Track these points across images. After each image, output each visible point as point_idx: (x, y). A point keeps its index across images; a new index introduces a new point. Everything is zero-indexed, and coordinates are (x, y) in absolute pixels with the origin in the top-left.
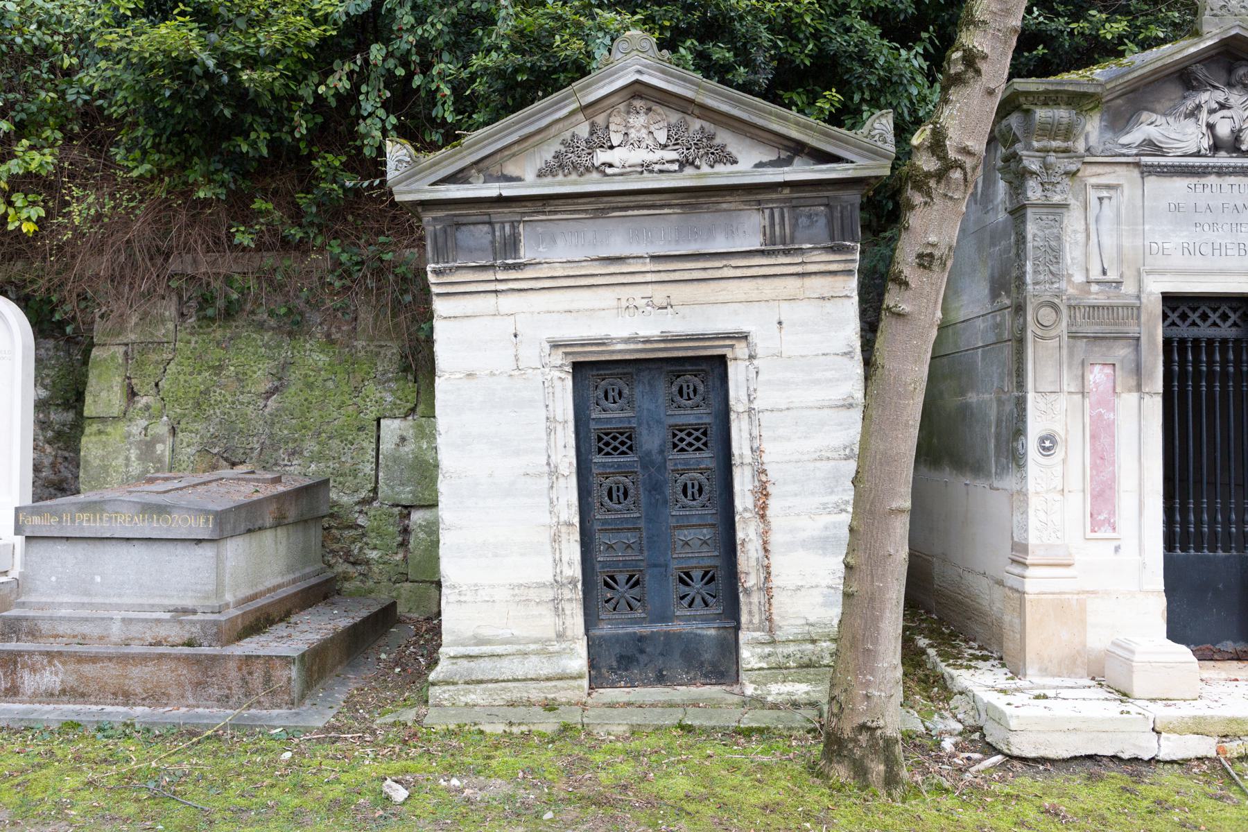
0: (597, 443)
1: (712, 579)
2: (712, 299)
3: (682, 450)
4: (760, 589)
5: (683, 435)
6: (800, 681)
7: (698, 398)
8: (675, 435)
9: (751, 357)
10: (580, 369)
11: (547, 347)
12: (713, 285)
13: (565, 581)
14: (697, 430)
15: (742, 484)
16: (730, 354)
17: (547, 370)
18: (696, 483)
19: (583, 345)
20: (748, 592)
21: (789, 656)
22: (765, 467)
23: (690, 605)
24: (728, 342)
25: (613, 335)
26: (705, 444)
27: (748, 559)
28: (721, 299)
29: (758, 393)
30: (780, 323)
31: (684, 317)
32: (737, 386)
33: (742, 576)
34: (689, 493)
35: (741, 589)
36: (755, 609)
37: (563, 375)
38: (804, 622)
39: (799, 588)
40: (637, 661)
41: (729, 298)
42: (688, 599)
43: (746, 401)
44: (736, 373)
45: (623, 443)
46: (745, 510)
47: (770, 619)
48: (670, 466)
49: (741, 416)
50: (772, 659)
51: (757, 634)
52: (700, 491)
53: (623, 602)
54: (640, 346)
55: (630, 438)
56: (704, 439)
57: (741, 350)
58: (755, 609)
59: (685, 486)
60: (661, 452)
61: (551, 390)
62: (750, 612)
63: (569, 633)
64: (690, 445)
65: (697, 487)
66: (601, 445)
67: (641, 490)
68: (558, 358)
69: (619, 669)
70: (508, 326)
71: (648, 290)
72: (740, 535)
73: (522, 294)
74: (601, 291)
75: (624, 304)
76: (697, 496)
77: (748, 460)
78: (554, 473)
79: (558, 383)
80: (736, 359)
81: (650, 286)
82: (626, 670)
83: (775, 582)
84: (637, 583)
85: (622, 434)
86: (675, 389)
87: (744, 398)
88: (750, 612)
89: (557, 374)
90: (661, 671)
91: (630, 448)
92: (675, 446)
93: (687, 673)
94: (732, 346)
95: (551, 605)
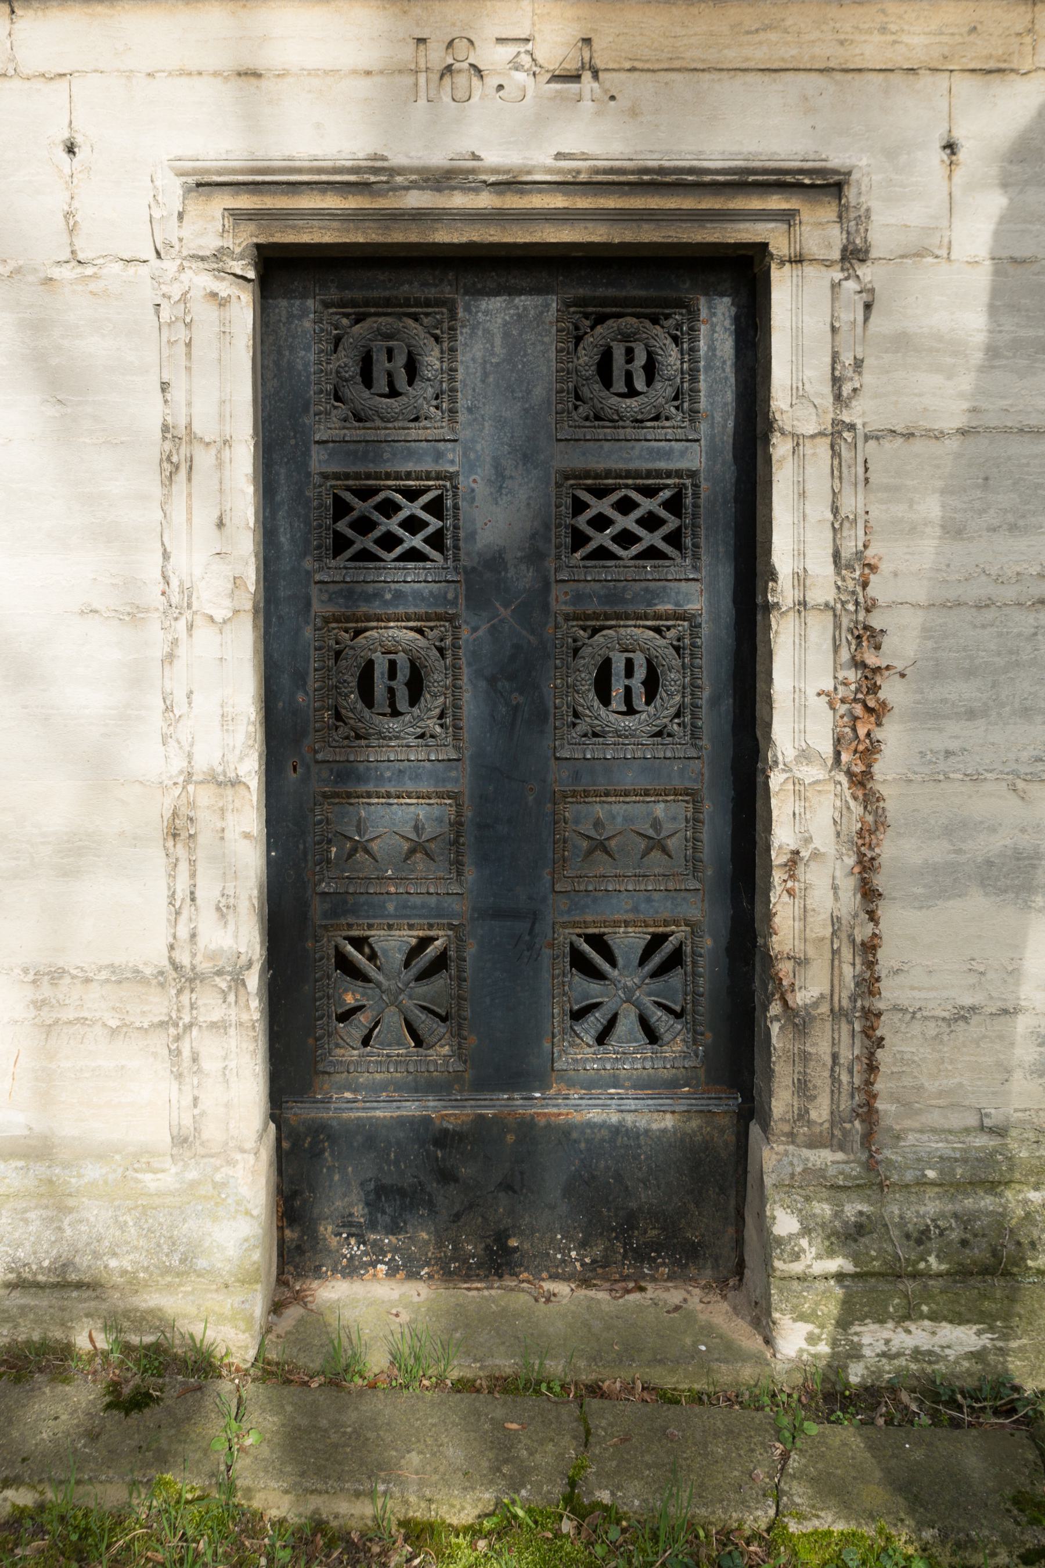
0: (331, 520)
1: (675, 959)
2: (732, 56)
3: (602, 554)
4: (837, 1014)
5: (604, 506)
6: (958, 1319)
7: (662, 390)
8: (579, 507)
9: (854, 255)
10: (280, 271)
11: (173, 190)
13: (204, 966)
14: (650, 492)
15: (801, 670)
16: (778, 241)
17: (170, 266)
18: (639, 660)
19: (294, 187)
20: (799, 1022)
21: (921, 1238)
22: (876, 621)
23: (602, 1039)
24: (776, 202)
25: (397, 159)
26: (674, 539)
27: (804, 909)
28: (759, 55)
29: (868, 378)
30: (950, 147)
31: (634, 112)
32: (798, 350)
33: (784, 968)
34: (617, 691)
35: (775, 1008)
36: (820, 1078)
37: (225, 288)
38: (972, 1121)
39: (963, 1015)
40: (431, 1205)
41: (787, 53)
42: (595, 1021)
43: (827, 401)
44: (798, 310)
45: (413, 525)
46: (805, 755)
47: (868, 1112)
48: (560, 601)
49: (808, 448)
50: (871, 1246)
51: (825, 1157)
52: (652, 685)
53: (393, 1019)
54: (485, 201)
55: (436, 507)
56: (672, 523)
57: (819, 229)
58: (820, 1078)
59: (605, 670)
60: (535, 556)
61: (182, 334)
62: (803, 1088)
63: (212, 1132)
64: (626, 538)
65: (640, 673)
66: (342, 526)
67: (465, 681)
68: (209, 227)
69: (373, 1226)
72: (783, 836)
75: (437, 57)
76: (639, 701)
77: (823, 588)
78: (180, 606)
79: (205, 314)
80: (798, 260)
82: (393, 1229)
83: (892, 992)
84: (441, 962)
85: (412, 495)
86: (586, 358)
87: (821, 390)
88: (803, 1088)
89: (203, 281)
90: (501, 1237)
91: (436, 540)
92: (579, 539)
93: (583, 1245)
94: (788, 217)
95: (159, 1042)
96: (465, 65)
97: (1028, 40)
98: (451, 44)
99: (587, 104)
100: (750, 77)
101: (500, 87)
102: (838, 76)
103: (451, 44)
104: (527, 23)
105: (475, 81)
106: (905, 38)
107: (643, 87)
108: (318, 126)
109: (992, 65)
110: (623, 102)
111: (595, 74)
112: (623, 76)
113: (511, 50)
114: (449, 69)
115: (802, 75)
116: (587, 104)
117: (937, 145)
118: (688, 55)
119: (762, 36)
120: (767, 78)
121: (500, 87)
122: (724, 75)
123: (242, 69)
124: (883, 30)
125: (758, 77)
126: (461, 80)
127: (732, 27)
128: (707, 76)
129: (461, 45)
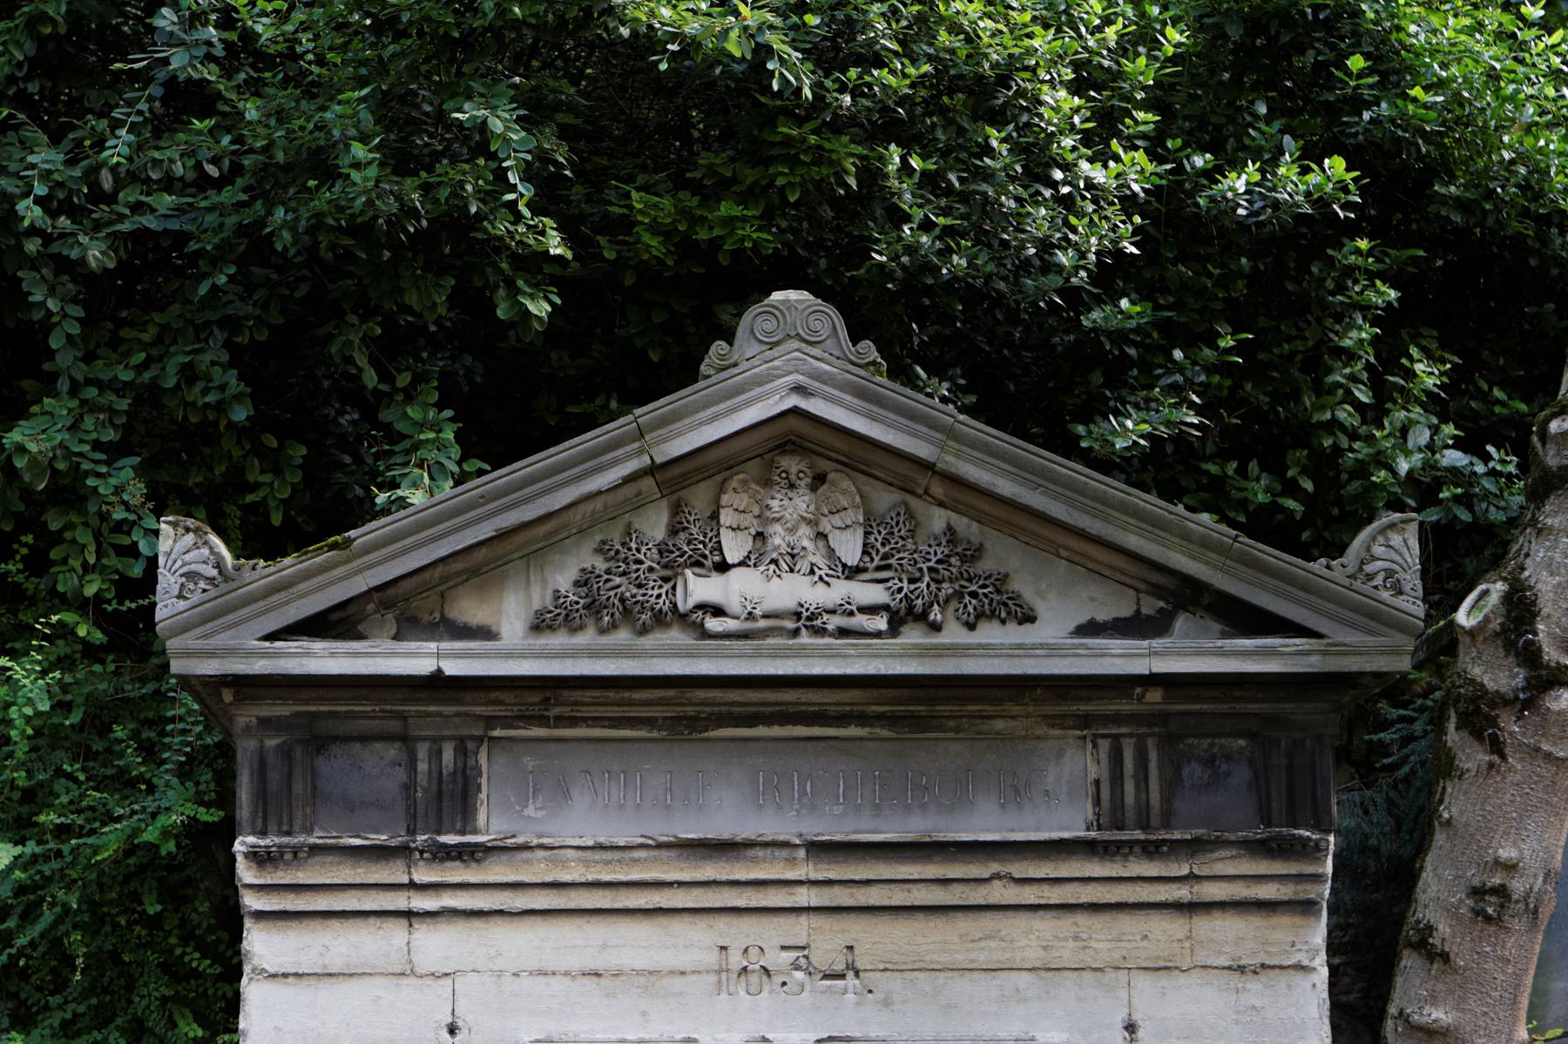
2: (961, 958)
12: (964, 923)
28: (982, 958)
70: (433, 1004)
71: (799, 930)
73: (477, 923)
74: (678, 925)
75: (736, 960)
81: (803, 919)
96: (757, 967)
97: (1187, 944)
98: (746, 950)
99: (850, 996)
100: (976, 975)
101: (784, 984)
102: (1044, 974)
103: (746, 950)
104: (804, 934)
105: (765, 978)
106: (1093, 944)
107: (894, 983)
108: (644, 1013)
109: (1161, 964)
110: (878, 995)
111: (857, 974)
112: (878, 974)
113: (793, 955)
114: (745, 969)
115: (1015, 973)
116: (850, 996)
117: (1120, 1026)
118: (928, 958)
119: (983, 944)
120: (988, 975)
121: (784, 984)
122: (956, 974)
123: (587, 970)
124: (1076, 938)
125: (982, 975)
126: (754, 979)
127: (961, 936)
128: (943, 975)
129: (753, 952)
